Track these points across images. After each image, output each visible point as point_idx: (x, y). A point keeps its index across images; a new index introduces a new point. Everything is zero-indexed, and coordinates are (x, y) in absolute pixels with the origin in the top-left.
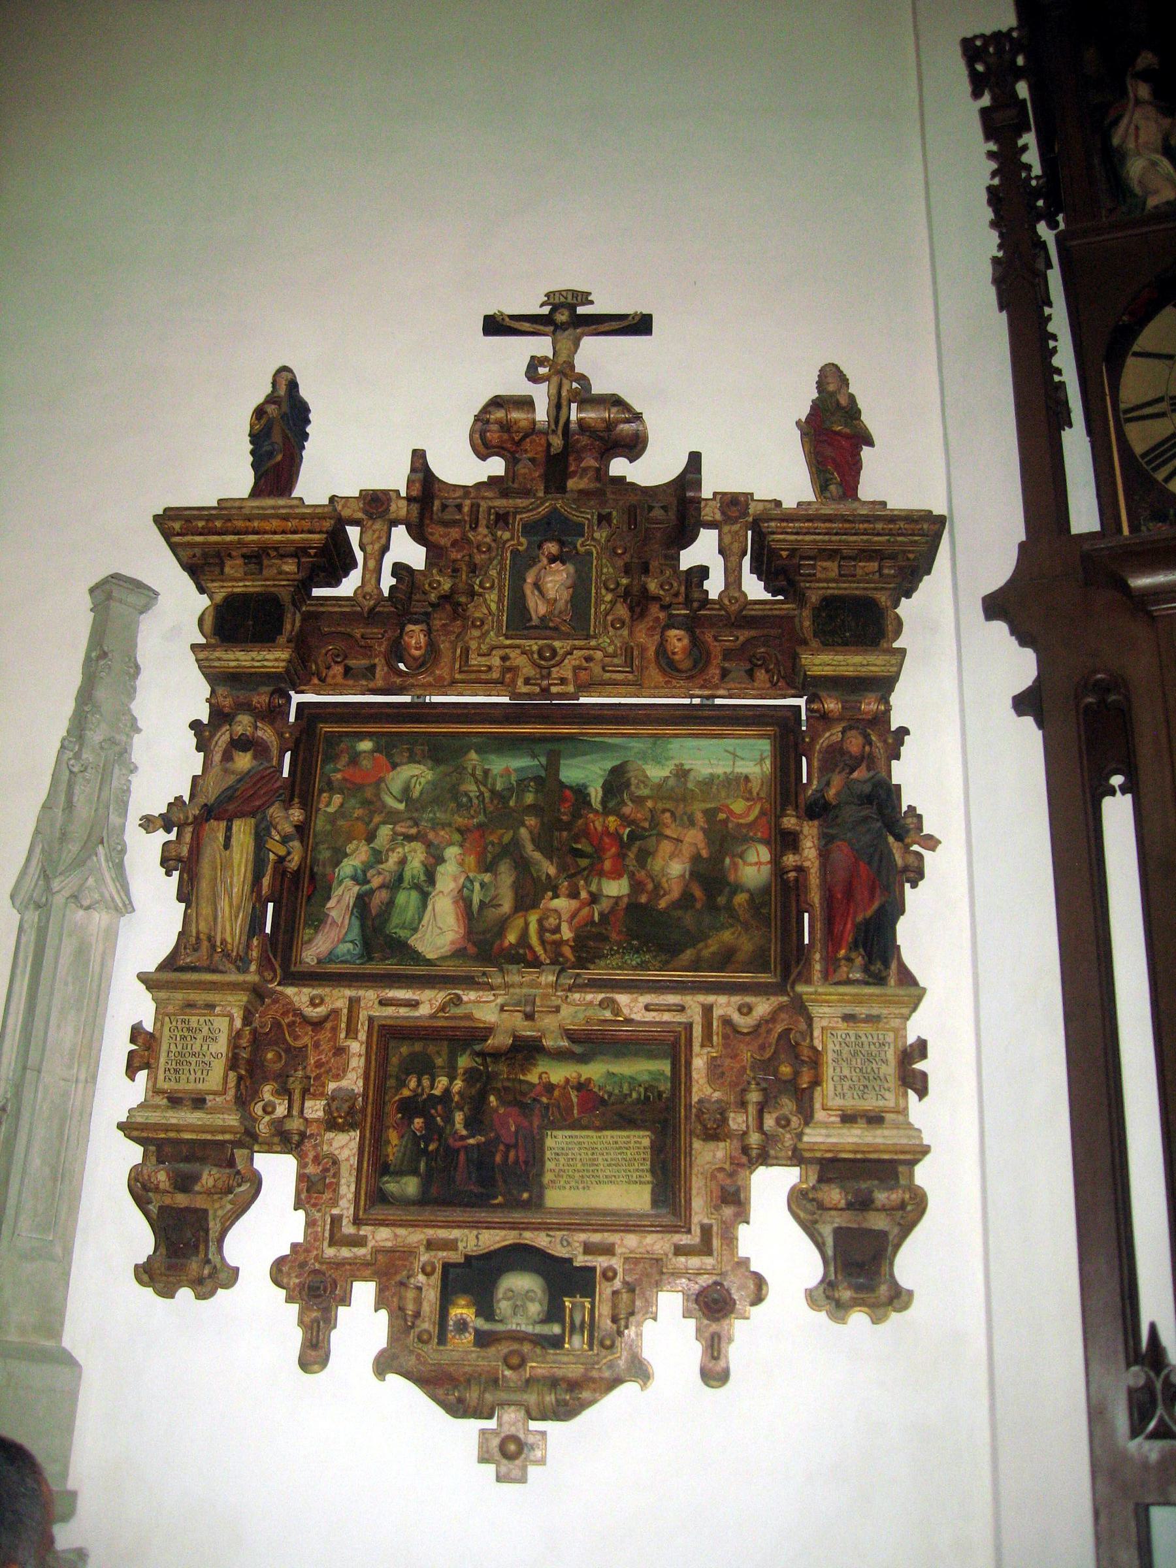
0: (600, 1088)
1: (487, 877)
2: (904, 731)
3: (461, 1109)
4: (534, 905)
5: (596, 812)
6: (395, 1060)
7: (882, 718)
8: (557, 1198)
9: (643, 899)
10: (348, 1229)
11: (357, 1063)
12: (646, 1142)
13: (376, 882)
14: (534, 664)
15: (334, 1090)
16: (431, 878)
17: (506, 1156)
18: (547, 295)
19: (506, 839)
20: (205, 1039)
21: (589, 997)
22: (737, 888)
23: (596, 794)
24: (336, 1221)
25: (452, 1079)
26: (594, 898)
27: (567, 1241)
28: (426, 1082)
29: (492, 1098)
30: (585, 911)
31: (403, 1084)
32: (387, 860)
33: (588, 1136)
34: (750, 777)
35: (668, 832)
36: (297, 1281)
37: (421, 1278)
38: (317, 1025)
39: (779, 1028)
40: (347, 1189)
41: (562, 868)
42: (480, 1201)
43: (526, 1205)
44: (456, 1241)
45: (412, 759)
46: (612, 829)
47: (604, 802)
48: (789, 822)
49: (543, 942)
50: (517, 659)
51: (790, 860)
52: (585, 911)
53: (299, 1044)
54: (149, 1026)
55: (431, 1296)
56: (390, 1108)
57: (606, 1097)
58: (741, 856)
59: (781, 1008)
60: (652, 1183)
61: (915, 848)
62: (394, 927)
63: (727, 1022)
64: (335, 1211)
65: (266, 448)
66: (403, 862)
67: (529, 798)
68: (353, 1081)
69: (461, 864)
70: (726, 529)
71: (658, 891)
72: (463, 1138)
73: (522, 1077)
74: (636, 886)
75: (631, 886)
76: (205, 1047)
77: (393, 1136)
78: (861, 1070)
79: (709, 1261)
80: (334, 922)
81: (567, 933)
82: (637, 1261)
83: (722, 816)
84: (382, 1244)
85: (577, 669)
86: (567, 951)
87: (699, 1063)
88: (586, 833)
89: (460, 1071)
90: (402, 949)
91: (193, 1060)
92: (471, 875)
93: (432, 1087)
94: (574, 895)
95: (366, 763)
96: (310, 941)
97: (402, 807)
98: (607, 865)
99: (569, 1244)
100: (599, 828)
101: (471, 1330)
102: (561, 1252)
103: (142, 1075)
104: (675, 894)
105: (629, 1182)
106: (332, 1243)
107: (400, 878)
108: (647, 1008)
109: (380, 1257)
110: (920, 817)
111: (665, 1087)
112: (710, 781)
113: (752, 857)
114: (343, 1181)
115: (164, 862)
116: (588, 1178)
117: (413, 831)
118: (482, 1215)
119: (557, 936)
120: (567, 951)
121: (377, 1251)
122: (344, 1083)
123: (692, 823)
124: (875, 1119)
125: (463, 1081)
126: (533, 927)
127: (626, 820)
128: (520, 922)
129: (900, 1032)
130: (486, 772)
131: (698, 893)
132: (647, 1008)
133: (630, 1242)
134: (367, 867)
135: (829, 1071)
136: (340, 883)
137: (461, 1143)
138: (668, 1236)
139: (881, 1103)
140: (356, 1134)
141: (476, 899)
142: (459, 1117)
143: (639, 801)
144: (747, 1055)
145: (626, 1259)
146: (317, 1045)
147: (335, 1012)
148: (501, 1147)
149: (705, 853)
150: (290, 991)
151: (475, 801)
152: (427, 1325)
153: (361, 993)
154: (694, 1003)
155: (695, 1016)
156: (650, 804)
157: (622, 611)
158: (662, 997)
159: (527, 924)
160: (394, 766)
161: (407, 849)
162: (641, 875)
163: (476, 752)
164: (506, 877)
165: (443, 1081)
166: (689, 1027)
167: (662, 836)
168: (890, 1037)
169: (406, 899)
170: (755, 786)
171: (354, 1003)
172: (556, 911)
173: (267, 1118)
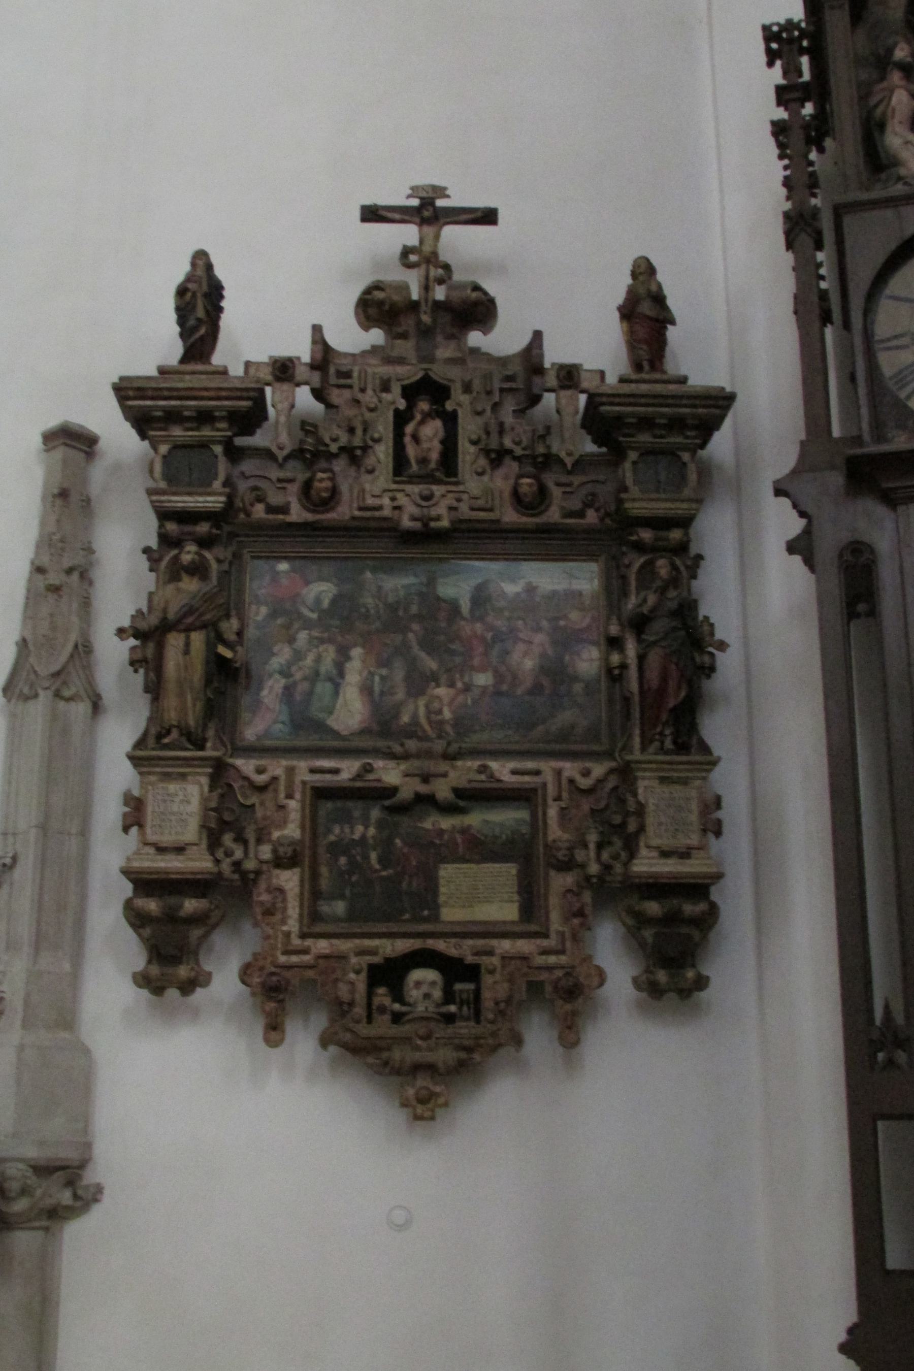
0: (478, 831)
1: (384, 672)
2: (700, 557)
3: (375, 850)
4: (421, 692)
5: (465, 619)
6: (322, 813)
7: (682, 548)
8: (451, 914)
9: (504, 687)
10: (296, 942)
12: (514, 872)
13: (298, 676)
15: (279, 838)
16: (341, 674)
17: (410, 883)
18: (412, 188)
20: (182, 801)
21: (469, 763)
22: (575, 678)
23: (465, 606)
24: (288, 935)
25: (366, 827)
26: (467, 688)
27: (459, 945)
28: (347, 830)
29: (398, 841)
30: (461, 699)
31: (329, 831)
32: (306, 658)
33: (471, 869)
34: (584, 593)
35: (521, 635)
36: (258, 980)
37: (352, 976)
38: (262, 789)
39: (611, 784)
40: (293, 911)
43: (426, 920)
44: (377, 947)
45: (321, 579)
46: (479, 632)
47: (472, 611)
48: (614, 630)
49: (430, 722)
50: (402, 500)
51: (615, 658)
52: (461, 699)
53: (248, 803)
54: (136, 793)
55: (361, 987)
56: (321, 850)
57: (483, 838)
58: (578, 655)
59: (611, 771)
60: (519, 901)
61: (711, 649)
62: (315, 712)
63: (571, 781)
64: (285, 928)
65: (192, 322)
66: (318, 659)
67: (414, 609)
68: (292, 830)
69: (363, 662)
70: (564, 394)
72: (376, 871)
73: (420, 825)
74: (499, 677)
75: (495, 677)
76: (182, 808)
77: (324, 870)
78: (673, 818)
79: (563, 959)
80: (268, 708)
81: (447, 714)
82: (512, 958)
83: (562, 623)
84: (323, 951)
85: (451, 509)
86: (449, 729)
87: (553, 812)
89: (373, 821)
90: (321, 727)
91: (173, 818)
92: (372, 669)
93: (352, 832)
94: (452, 685)
95: (284, 581)
97: (314, 616)
98: (476, 662)
99: (461, 947)
100: (469, 632)
101: (389, 1012)
102: (453, 952)
103: (134, 830)
104: (528, 683)
105: (501, 901)
106: (286, 952)
107: (317, 673)
108: (514, 772)
109: (321, 961)
110: (712, 625)
111: (525, 829)
112: (553, 595)
113: (585, 655)
114: (290, 905)
115: (132, 663)
117: (326, 635)
118: (394, 928)
119: (439, 717)
120: (449, 729)
122: (286, 832)
123: (538, 629)
124: (685, 854)
125: (374, 828)
126: (422, 711)
128: (410, 707)
130: (380, 588)
131: (546, 682)
132: (514, 772)
133: (506, 945)
134: (290, 664)
135: (650, 820)
136: (270, 676)
137: (376, 875)
138: (533, 941)
139: (689, 842)
140: (297, 871)
141: (377, 688)
142: (373, 856)
145: (503, 958)
146: (262, 804)
147: (275, 779)
148: (407, 877)
149: (550, 652)
150: (239, 762)
151: (372, 611)
152: (359, 1011)
153: (294, 763)
154: (547, 767)
155: (548, 777)
156: (507, 614)
157: (483, 462)
158: (523, 763)
159: (417, 708)
160: (307, 583)
161: (321, 649)
162: (503, 669)
163: (371, 572)
165: (359, 829)
166: (545, 785)
167: (517, 640)
168: (694, 793)
169: (323, 688)
171: (290, 771)
172: (438, 697)
173: (228, 860)
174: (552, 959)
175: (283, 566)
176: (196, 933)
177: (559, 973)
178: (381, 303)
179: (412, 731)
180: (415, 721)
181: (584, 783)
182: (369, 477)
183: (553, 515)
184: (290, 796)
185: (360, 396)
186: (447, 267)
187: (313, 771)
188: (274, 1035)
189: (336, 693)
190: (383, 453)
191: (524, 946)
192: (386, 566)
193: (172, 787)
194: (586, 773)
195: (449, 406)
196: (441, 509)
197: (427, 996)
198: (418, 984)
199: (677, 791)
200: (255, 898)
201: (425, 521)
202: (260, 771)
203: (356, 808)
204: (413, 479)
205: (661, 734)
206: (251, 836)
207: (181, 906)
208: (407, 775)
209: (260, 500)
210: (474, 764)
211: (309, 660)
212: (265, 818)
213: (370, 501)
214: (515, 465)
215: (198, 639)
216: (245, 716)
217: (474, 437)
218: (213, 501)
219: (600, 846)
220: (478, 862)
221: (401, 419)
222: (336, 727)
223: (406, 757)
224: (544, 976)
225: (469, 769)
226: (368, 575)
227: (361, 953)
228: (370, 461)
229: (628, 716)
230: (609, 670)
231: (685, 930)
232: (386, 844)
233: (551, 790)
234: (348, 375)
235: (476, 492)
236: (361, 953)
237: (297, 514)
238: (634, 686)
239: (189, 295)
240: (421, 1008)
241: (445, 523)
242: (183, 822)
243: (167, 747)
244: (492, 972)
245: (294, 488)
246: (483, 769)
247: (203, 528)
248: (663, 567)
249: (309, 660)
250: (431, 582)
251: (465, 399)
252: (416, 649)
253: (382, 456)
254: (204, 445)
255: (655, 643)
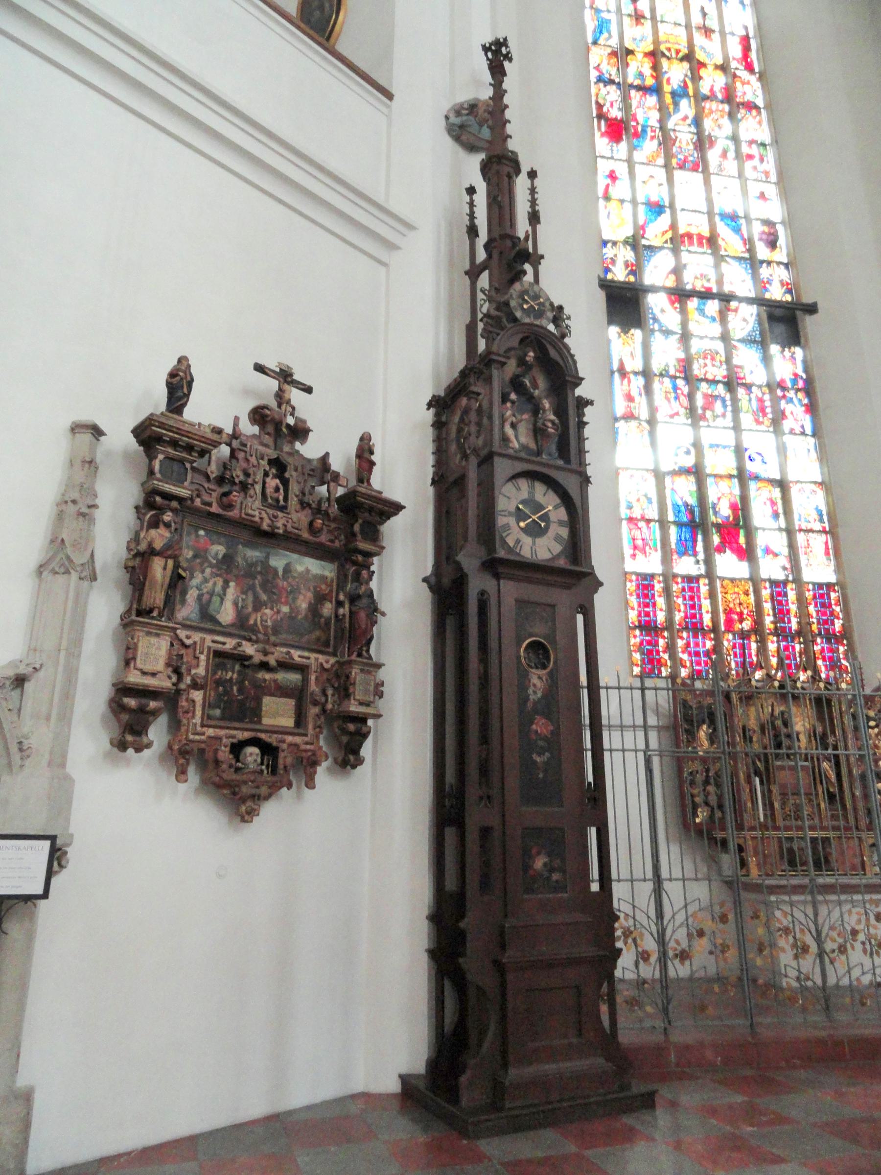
1: (244, 597)
8: (266, 721)
10: (199, 728)
11: (203, 663)
13: (205, 591)
14: (270, 519)
16: (225, 595)
19: (251, 583)
22: (321, 616)
23: (280, 573)
24: (195, 725)
25: (233, 673)
26: (278, 612)
37: (223, 748)
38: (186, 647)
39: (334, 669)
40: (199, 713)
41: (269, 598)
42: (241, 720)
43: (255, 723)
45: (220, 544)
47: (283, 576)
48: (342, 597)
49: (262, 625)
50: (264, 515)
52: (275, 617)
59: (337, 662)
62: (212, 610)
63: (322, 664)
64: (194, 721)
66: (215, 584)
67: (259, 569)
68: (201, 671)
71: (298, 612)
81: (269, 623)
87: (313, 677)
88: (276, 586)
90: (214, 620)
94: (272, 609)
95: (202, 541)
96: (179, 610)
97: (215, 562)
98: (283, 600)
102: (269, 740)
107: (214, 591)
108: (300, 656)
116: (275, 715)
121: (210, 737)
123: (309, 590)
124: (368, 704)
127: (290, 584)
129: (375, 677)
130: (245, 555)
132: (300, 656)
133: (290, 739)
134: (202, 583)
141: (240, 605)
142: (235, 688)
143: (294, 578)
144: (325, 676)
146: (187, 654)
153: (205, 636)
154: (313, 656)
155: (312, 661)
157: (298, 507)
160: (213, 544)
164: (250, 599)
165: (230, 674)
167: (300, 593)
169: (216, 600)
170: (329, 580)
171: (203, 640)
174: (308, 747)
175: (202, 533)
176: (151, 718)
177: (310, 754)
178: (267, 416)
179: (253, 629)
180: (255, 624)
181: (327, 666)
182: (251, 500)
183: (324, 538)
184: (202, 653)
185: (249, 458)
186: (293, 408)
187: (213, 641)
188: (182, 777)
189: (222, 603)
190: (258, 488)
191: (298, 740)
192: (248, 544)
193: (154, 640)
194: (327, 662)
195: (287, 475)
196: (279, 524)
197: (255, 761)
198: (251, 754)
199: (368, 677)
200: (180, 704)
201: (272, 527)
202: (188, 637)
203: (229, 663)
204: (270, 506)
205: (361, 649)
206: (183, 670)
207: (148, 705)
208: (258, 651)
209: (198, 496)
210: (284, 650)
211: (210, 585)
212: (188, 662)
213: (250, 512)
214: (310, 511)
215: (170, 563)
216: (178, 607)
217: (297, 493)
218: (183, 492)
219: (333, 695)
220: (280, 697)
221: (266, 474)
222: (221, 620)
223: (257, 642)
224: (304, 754)
225: (282, 652)
226: (240, 546)
227: (228, 737)
228: (252, 492)
229: (342, 638)
230: (337, 616)
231: (358, 738)
232: (240, 683)
233: (313, 667)
234: (245, 445)
235: (295, 519)
236: (228, 737)
237: (215, 509)
238: (347, 625)
239: (178, 378)
240: (251, 766)
241: (281, 531)
242: (156, 659)
243: (153, 618)
244: (283, 751)
245: (214, 494)
246: (288, 653)
247: (174, 504)
248: (364, 573)
249: (210, 585)
250: (267, 557)
251: (294, 474)
252: (258, 589)
253: (258, 492)
254: (181, 461)
255: (363, 608)
